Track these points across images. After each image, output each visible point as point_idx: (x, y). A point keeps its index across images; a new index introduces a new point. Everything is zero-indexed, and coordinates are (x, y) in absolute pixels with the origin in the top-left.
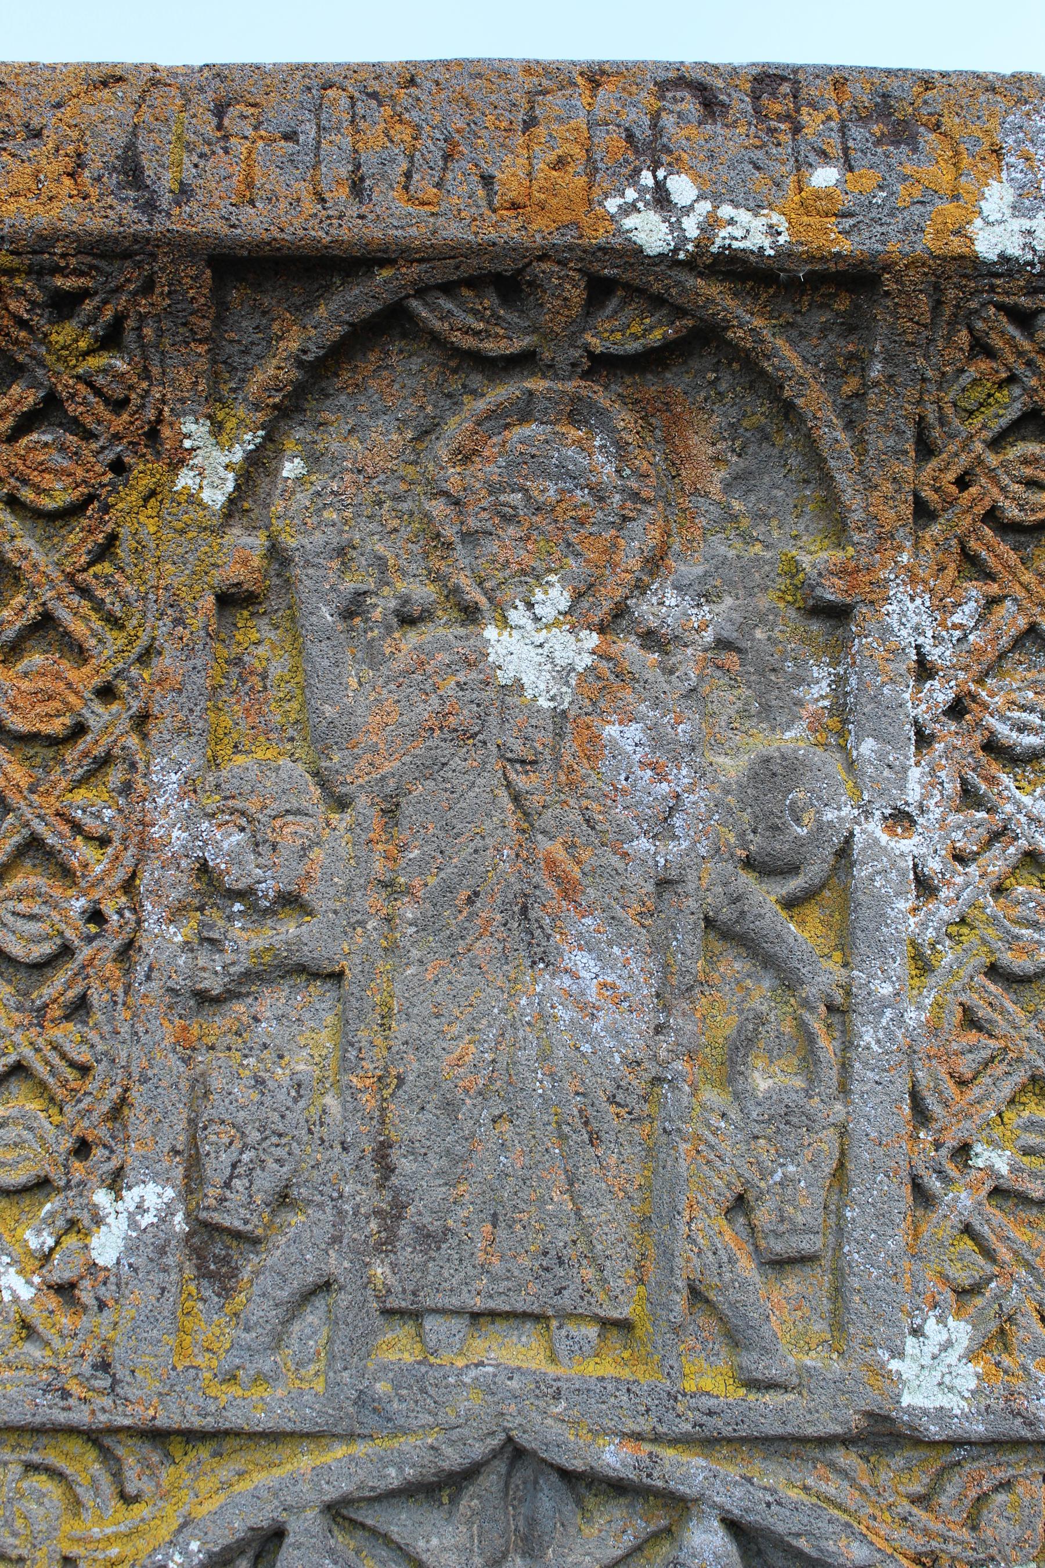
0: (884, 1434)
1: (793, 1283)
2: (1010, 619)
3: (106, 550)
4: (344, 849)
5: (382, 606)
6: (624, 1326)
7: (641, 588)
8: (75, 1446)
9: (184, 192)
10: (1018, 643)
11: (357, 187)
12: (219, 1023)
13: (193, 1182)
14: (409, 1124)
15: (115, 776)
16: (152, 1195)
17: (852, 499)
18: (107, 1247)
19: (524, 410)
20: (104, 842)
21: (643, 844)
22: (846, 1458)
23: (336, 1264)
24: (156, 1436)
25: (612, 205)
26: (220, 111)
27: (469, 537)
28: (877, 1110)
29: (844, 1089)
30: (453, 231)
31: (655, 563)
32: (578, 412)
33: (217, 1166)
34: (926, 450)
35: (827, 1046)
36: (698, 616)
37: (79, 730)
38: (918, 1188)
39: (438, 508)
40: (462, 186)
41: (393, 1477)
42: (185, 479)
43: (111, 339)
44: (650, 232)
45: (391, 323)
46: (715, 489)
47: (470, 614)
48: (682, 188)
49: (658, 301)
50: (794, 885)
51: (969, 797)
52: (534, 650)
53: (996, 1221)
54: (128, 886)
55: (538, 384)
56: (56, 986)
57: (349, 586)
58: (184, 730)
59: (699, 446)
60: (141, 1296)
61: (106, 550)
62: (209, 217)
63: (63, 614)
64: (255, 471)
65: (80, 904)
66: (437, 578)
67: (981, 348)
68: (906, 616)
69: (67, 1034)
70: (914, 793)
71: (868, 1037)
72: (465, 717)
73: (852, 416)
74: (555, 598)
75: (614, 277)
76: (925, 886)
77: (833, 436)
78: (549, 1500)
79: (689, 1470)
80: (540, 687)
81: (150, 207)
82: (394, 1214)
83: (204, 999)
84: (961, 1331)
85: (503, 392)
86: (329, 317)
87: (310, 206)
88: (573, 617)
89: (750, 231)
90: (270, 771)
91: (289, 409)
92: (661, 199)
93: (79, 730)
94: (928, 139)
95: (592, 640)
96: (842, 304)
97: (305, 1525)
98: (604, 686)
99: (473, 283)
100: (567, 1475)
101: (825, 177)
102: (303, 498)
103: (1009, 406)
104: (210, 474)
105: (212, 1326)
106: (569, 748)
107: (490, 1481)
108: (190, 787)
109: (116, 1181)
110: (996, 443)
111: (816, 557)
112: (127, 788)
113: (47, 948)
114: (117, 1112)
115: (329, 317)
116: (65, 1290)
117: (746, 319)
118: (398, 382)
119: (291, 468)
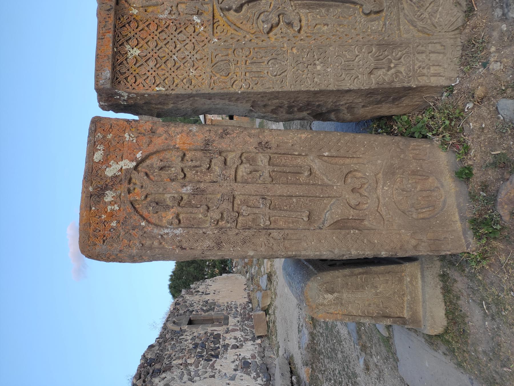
9: (111, 6)
12: (181, 14)
13: (194, 14)
18: (199, 21)
24: (213, 19)
33: (193, 12)
42: (135, 13)
43: (123, 17)
54: (170, 20)
56: (178, 25)
60: (203, 18)
64: (135, 8)
69: (182, 25)
83: (179, 14)
90: (160, 9)
105: (205, 14)
108: (162, 14)
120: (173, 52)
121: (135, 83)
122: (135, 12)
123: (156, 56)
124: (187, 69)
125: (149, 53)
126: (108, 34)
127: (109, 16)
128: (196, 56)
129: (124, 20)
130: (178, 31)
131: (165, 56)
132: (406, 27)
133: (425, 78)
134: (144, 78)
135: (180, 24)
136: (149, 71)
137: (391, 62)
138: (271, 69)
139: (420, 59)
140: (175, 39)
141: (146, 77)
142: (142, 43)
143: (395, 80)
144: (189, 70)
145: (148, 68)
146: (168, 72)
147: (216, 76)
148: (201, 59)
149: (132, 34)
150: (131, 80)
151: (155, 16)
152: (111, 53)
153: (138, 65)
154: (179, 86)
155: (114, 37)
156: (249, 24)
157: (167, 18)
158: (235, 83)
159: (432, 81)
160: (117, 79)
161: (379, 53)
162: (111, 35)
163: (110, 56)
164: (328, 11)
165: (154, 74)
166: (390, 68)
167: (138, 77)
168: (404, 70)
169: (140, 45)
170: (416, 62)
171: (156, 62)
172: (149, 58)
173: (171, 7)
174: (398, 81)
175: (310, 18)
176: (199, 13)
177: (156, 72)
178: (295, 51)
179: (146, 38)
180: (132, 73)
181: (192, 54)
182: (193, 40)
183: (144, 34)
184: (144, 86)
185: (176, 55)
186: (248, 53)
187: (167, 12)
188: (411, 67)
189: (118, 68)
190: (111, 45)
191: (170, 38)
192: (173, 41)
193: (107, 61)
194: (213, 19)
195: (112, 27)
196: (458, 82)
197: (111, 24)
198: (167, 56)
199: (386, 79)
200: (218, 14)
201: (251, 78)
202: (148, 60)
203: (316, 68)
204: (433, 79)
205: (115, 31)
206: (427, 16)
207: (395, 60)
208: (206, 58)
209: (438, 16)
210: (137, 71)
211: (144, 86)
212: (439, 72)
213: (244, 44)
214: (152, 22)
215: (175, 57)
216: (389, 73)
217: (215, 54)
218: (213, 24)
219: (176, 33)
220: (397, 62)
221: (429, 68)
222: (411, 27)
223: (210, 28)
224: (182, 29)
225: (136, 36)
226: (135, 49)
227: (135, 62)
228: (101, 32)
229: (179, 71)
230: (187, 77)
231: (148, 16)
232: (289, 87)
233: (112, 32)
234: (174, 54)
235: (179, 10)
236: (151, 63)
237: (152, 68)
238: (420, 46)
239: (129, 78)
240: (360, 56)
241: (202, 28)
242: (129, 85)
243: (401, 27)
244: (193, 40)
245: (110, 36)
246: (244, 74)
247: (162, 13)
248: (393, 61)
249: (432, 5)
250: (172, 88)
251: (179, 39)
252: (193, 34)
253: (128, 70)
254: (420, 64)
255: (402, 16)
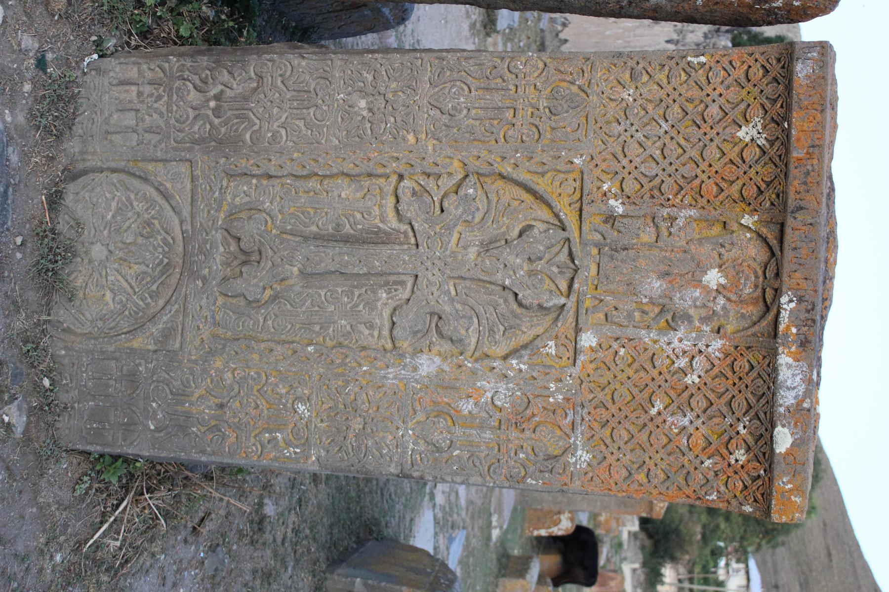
0: (578, 330)
1: (602, 317)
2: (716, 362)
3: (735, 201)
4: (679, 244)
5: (722, 250)
6: (596, 288)
7: (724, 297)
8: (579, 196)
9: (795, 218)
10: (712, 363)
11: (795, 249)
12: (649, 221)
14: (632, 253)
15: (694, 203)
16: (620, 210)
17: (739, 335)
18: (612, 202)
19: (757, 277)
20: (682, 201)
21: (678, 295)
22: (574, 324)
23: (608, 241)
24: (581, 210)
25: (789, 293)
26: (811, 224)
27: (734, 267)
28: (631, 332)
29: (635, 327)
30: (786, 265)
31: (729, 299)
32: (756, 286)
33: (625, 221)
34: (748, 348)
35: (642, 325)
36: (719, 307)
37: (702, 197)
38: (618, 339)
39: (740, 261)
40: (795, 267)
41: (574, 250)
42: (747, 216)
43: (772, 204)
44: (784, 299)
45: (773, 254)
46: (743, 311)
47: (720, 267)
48: (792, 305)
49: (774, 300)
50: (670, 321)
51: (684, 352)
52: (713, 278)
53: (612, 351)
54: (674, 206)
55: (761, 279)
56: (656, 193)
57: (726, 245)
58: (701, 215)
59: (751, 308)
60: (604, 208)
61: (735, 201)
62: (790, 222)
63: (723, 194)
65: (671, 197)
66: (727, 261)
67: (764, 357)
68: (717, 344)
69: (648, 195)
70: (686, 343)
71: (643, 332)
72: (701, 265)
73: (754, 335)
74: (723, 281)
75: (778, 293)
76: (669, 344)
77: (750, 332)
78: (569, 275)
79: (573, 298)
80: (706, 278)
81: (792, 212)
82: (616, 250)
83: (654, 218)
84: (594, 344)
85: (760, 273)
86: (774, 243)
87: (792, 240)
88: (719, 285)
89: (785, 316)
91: (759, 235)
92: (791, 301)
93: (702, 197)
94: (801, 349)
95: (715, 288)
96: (773, 333)
97: (565, 234)
98: (706, 289)
99: (778, 269)
100: (573, 279)
101: (794, 330)
102: (743, 237)
103: (754, 363)
104: (747, 220)
106: (696, 283)
107: (572, 265)
108: (690, 216)
109: (623, 203)
110: (748, 361)
111: (730, 329)
112: (691, 205)
113: (663, 190)
114: (634, 203)
115: (774, 243)
116: (605, 194)
117: (771, 316)
118: (762, 255)
119: (748, 235)
120: (668, 137)
121: (750, 67)
122: (747, 220)
123: (705, 128)
124: (640, 102)
125: (718, 134)
126: (800, 156)
127: (798, 196)
128: (621, 128)
129: (770, 195)
130: (657, 181)
131: (687, 127)
132: (179, 186)
133: (149, 75)
134: (730, 79)
135: (653, 197)
136: (721, 95)
137: (217, 112)
138: (462, 100)
139: (155, 116)
140: (664, 164)
141: (726, 82)
142: (733, 154)
143: (209, 73)
144: (635, 100)
145: (722, 100)
146: (680, 95)
147: (580, 87)
148: (608, 123)
149: (753, 171)
150: (757, 72)
151: (705, 213)
152: (795, 114)
153: (743, 106)
154: (658, 68)
155: (788, 152)
156: (506, 198)
157: (680, 209)
158: (539, 71)
159: (135, 69)
160: (783, 67)
161: (237, 129)
162: (795, 154)
163: (795, 107)
164: (338, 225)
165: (709, 90)
166: (218, 97)
167: (743, 80)
168: (189, 91)
169: (737, 149)
170: (164, 110)
171: (705, 114)
172: (718, 123)
173: (670, 234)
174: (203, 70)
175: (376, 211)
176: (612, 221)
177: (704, 93)
178: (411, 138)
179: (726, 164)
180: (755, 85)
181: (628, 134)
182: (625, 162)
183: (730, 172)
184: (731, 63)
185: (662, 131)
186: (510, 133)
187: (680, 222)
188: (175, 97)
189: (781, 87)
190: (793, 132)
191: (673, 167)
192: (668, 161)
193: (802, 97)
194: (581, 210)
195: (793, 172)
196: (87, 60)
197: (795, 179)
198: (682, 129)
199: (225, 76)
200: (570, 217)
201: (504, 81)
202: (720, 120)
203: (367, 102)
204: (133, 73)
205: (786, 165)
206: (135, 204)
207: (208, 116)
208: (598, 125)
209: (114, 204)
210: (744, 92)
211: (731, 63)
212: (120, 88)
213: (517, 152)
214: (712, 199)
215: (665, 126)
216: (221, 87)
217: (579, 131)
218: (582, 196)
219: (662, 176)
220: (203, 111)
221: (140, 94)
222: (169, 185)
223: (588, 186)
224: (647, 187)
225: (745, 167)
226: (748, 139)
227: (749, 110)
228: (815, 162)
229: (657, 97)
230: (639, 85)
231: (719, 211)
232: (426, 59)
233: (792, 160)
234: (666, 132)
235: (653, 230)
236: (714, 110)
237: (714, 101)
238: (153, 142)
239: (761, 74)
240: (276, 124)
241: (605, 187)
242: (761, 59)
243: (189, 186)
244: (625, 162)
245: (797, 153)
246: (519, 90)
247: (690, 220)
248: (210, 113)
249: (125, 227)
250: (673, 62)
251: (654, 165)
252: (626, 175)
253: (762, 91)
254: (156, 105)
255: (186, 213)
